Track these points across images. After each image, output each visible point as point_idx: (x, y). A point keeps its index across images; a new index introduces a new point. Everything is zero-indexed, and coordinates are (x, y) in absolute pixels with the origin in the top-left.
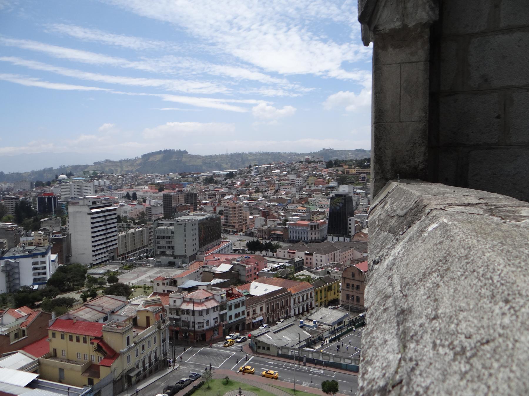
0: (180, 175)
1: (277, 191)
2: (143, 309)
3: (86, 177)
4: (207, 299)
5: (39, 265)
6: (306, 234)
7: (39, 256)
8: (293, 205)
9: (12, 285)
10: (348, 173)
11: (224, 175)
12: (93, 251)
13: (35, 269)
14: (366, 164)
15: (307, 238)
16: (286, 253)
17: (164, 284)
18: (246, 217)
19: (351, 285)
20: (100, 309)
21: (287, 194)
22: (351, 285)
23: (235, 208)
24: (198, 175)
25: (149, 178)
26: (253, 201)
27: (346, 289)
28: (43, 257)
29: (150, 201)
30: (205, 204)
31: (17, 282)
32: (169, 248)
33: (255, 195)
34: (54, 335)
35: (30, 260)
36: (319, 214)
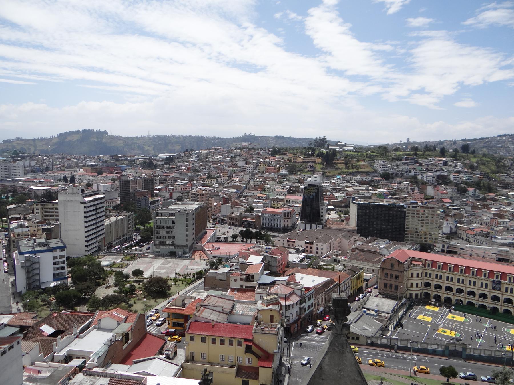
0: (113, 157)
1: (230, 177)
2: (265, 308)
3: (6, 156)
4: (291, 294)
5: (59, 260)
6: (279, 221)
7: (58, 250)
8: (250, 191)
9: (31, 281)
10: (295, 162)
11: (162, 159)
12: (86, 241)
13: (54, 264)
14: (310, 153)
15: (280, 225)
16: (286, 242)
17: (242, 280)
18: (211, 204)
19: (389, 275)
20: (220, 309)
21: (241, 181)
22: (389, 275)
23: (203, 195)
24: (134, 158)
25: (78, 159)
26: (208, 188)
27: (383, 278)
28: (62, 251)
29: (98, 186)
30: (159, 189)
31: (37, 278)
32: (169, 237)
33: (208, 181)
34: (192, 339)
35: (50, 254)
36: (279, 202)
